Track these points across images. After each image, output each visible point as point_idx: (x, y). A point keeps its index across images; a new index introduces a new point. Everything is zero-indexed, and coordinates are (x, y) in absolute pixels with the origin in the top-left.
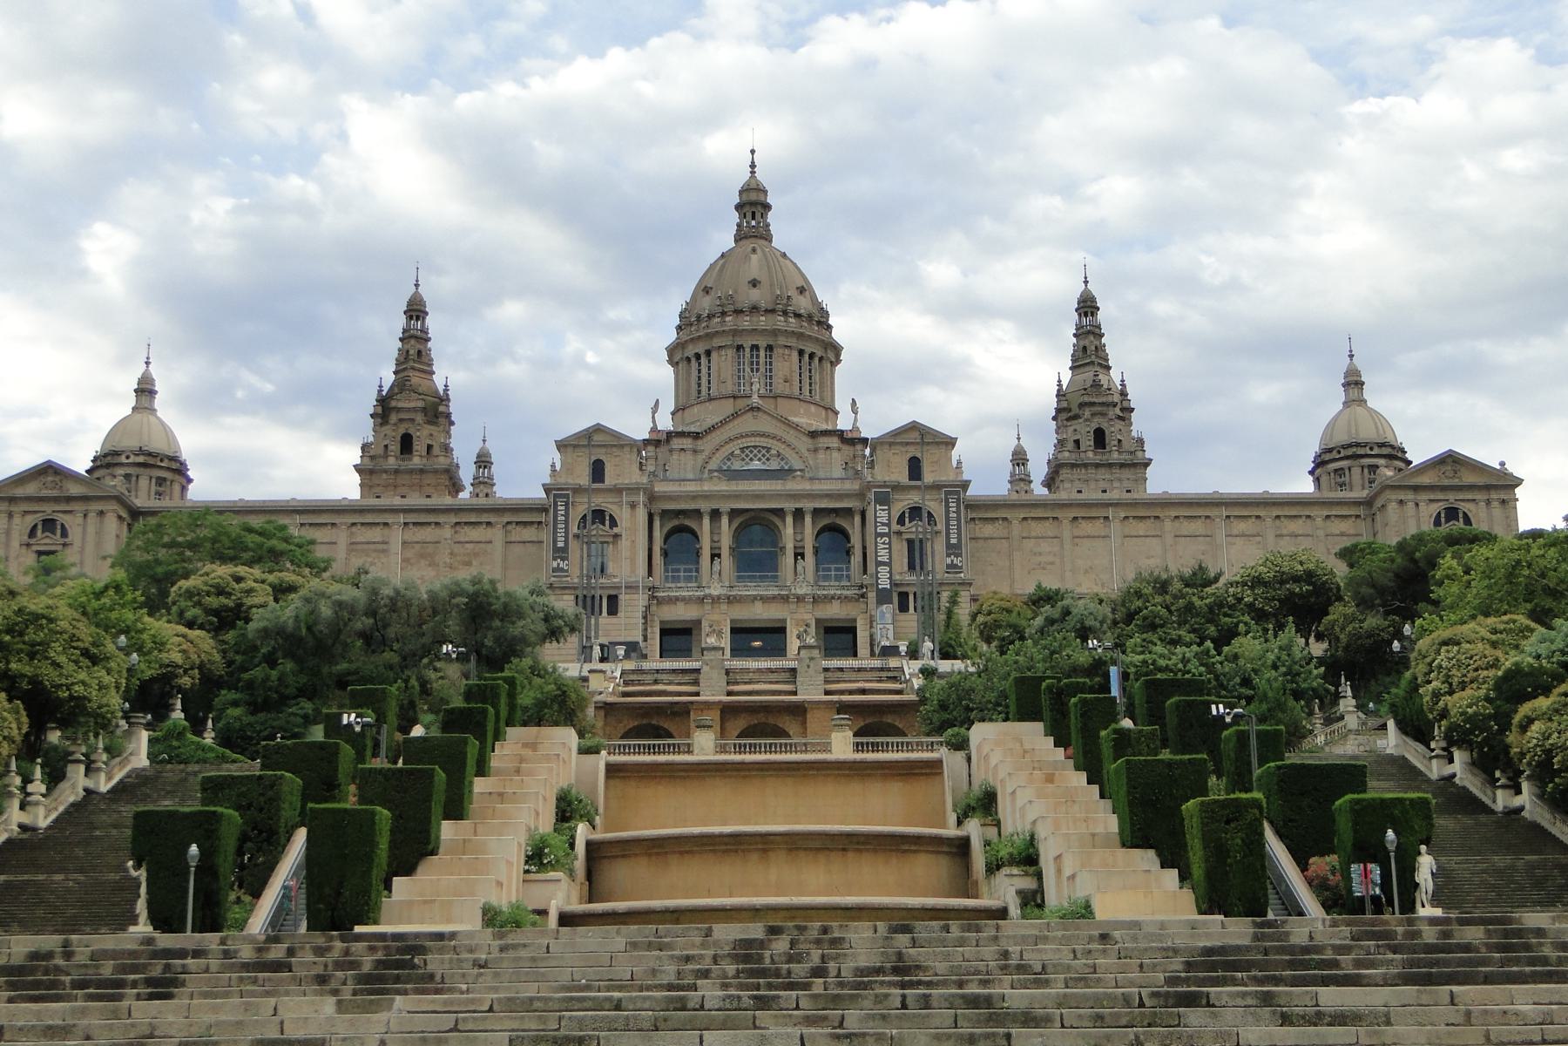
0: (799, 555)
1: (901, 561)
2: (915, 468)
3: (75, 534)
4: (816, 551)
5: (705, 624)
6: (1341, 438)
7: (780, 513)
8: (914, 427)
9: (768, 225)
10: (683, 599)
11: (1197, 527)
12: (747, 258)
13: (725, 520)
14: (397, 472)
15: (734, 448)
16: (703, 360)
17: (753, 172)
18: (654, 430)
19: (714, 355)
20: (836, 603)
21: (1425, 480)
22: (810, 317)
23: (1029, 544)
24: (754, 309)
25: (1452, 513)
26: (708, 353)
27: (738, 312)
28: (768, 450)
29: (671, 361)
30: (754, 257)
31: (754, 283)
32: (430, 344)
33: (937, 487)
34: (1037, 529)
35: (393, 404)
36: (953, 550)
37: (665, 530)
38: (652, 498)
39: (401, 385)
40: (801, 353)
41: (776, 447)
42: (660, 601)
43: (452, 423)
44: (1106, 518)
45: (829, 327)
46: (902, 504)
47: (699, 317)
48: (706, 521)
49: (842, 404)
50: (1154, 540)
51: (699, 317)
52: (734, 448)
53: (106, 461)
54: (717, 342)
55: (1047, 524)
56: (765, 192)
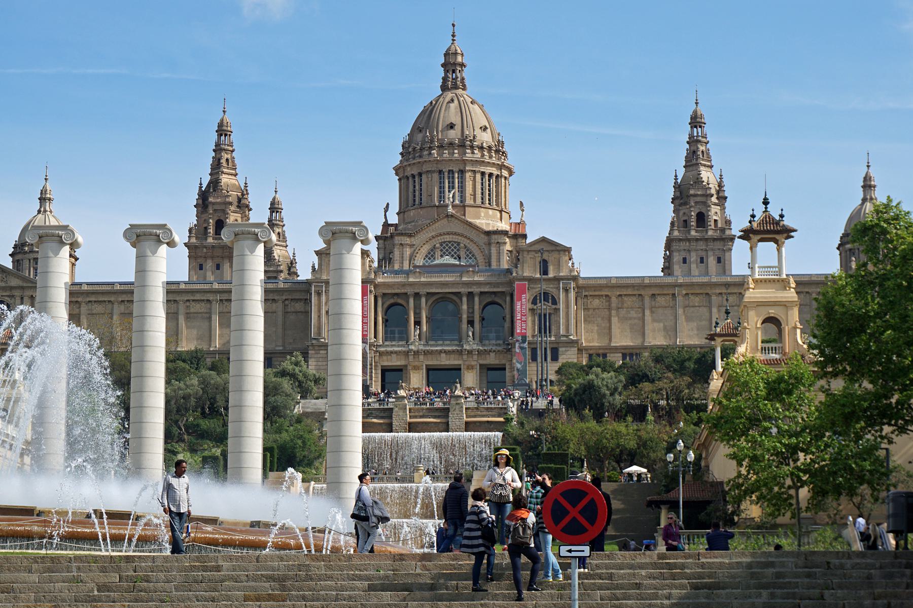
0: (471, 323)
4: (483, 319)
5: (409, 368)
7: (458, 294)
8: (543, 240)
9: (463, 79)
10: (396, 352)
12: (447, 108)
13: (423, 300)
14: (213, 247)
15: (437, 242)
16: (417, 179)
17: (453, 40)
18: (386, 225)
19: (424, 176)
20: (492, 355)
22: (490, 147)
23: (623, 312)
24: (451, 144)
26: (420, 174)
27: (441, 147)
28: (459, 244)
29: (397, 174)
30: (452, 105)
31: (452, 126)
32: (234, 154)
33: (557, 279)
34: (628, 301)
35: (211, 199)
37: (386, 306)
38: (376, 286)
39: (215, 183)
40: (483, 174)
41: (464, 242)
42: (381, 354)
43: (251, 210)
44: (674, 295)
45: (503, 153)
47: (414, 149)
48: (411, 301)
49: (512, 206)
50: (704, 310)
51: (414, 149)
54: (425, 168)
55: (634, 299)
56: (462, 55)
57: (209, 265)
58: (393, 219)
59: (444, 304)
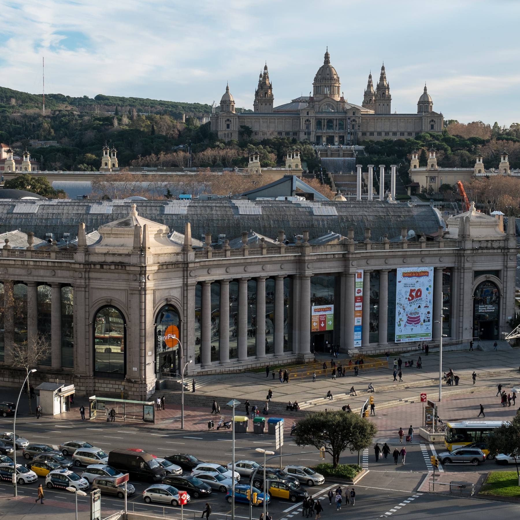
0: (336, 126)
1: (351, 128)
2: (354, 113)
3: (232, 120)
6: (422, 100)
11: (395, 120)
21: (429, 115)
25: (432, 121)
27: (325, 79)
31: (328, 74)
34: (372, 120)
36: (359, 126)
41: (331, 104)
46: (352, 119)
50: (389, 123)
52: (325, 104)
53: (222, 102)
57: (264, 104)
58: (312, 96)
59: (330, 121)
